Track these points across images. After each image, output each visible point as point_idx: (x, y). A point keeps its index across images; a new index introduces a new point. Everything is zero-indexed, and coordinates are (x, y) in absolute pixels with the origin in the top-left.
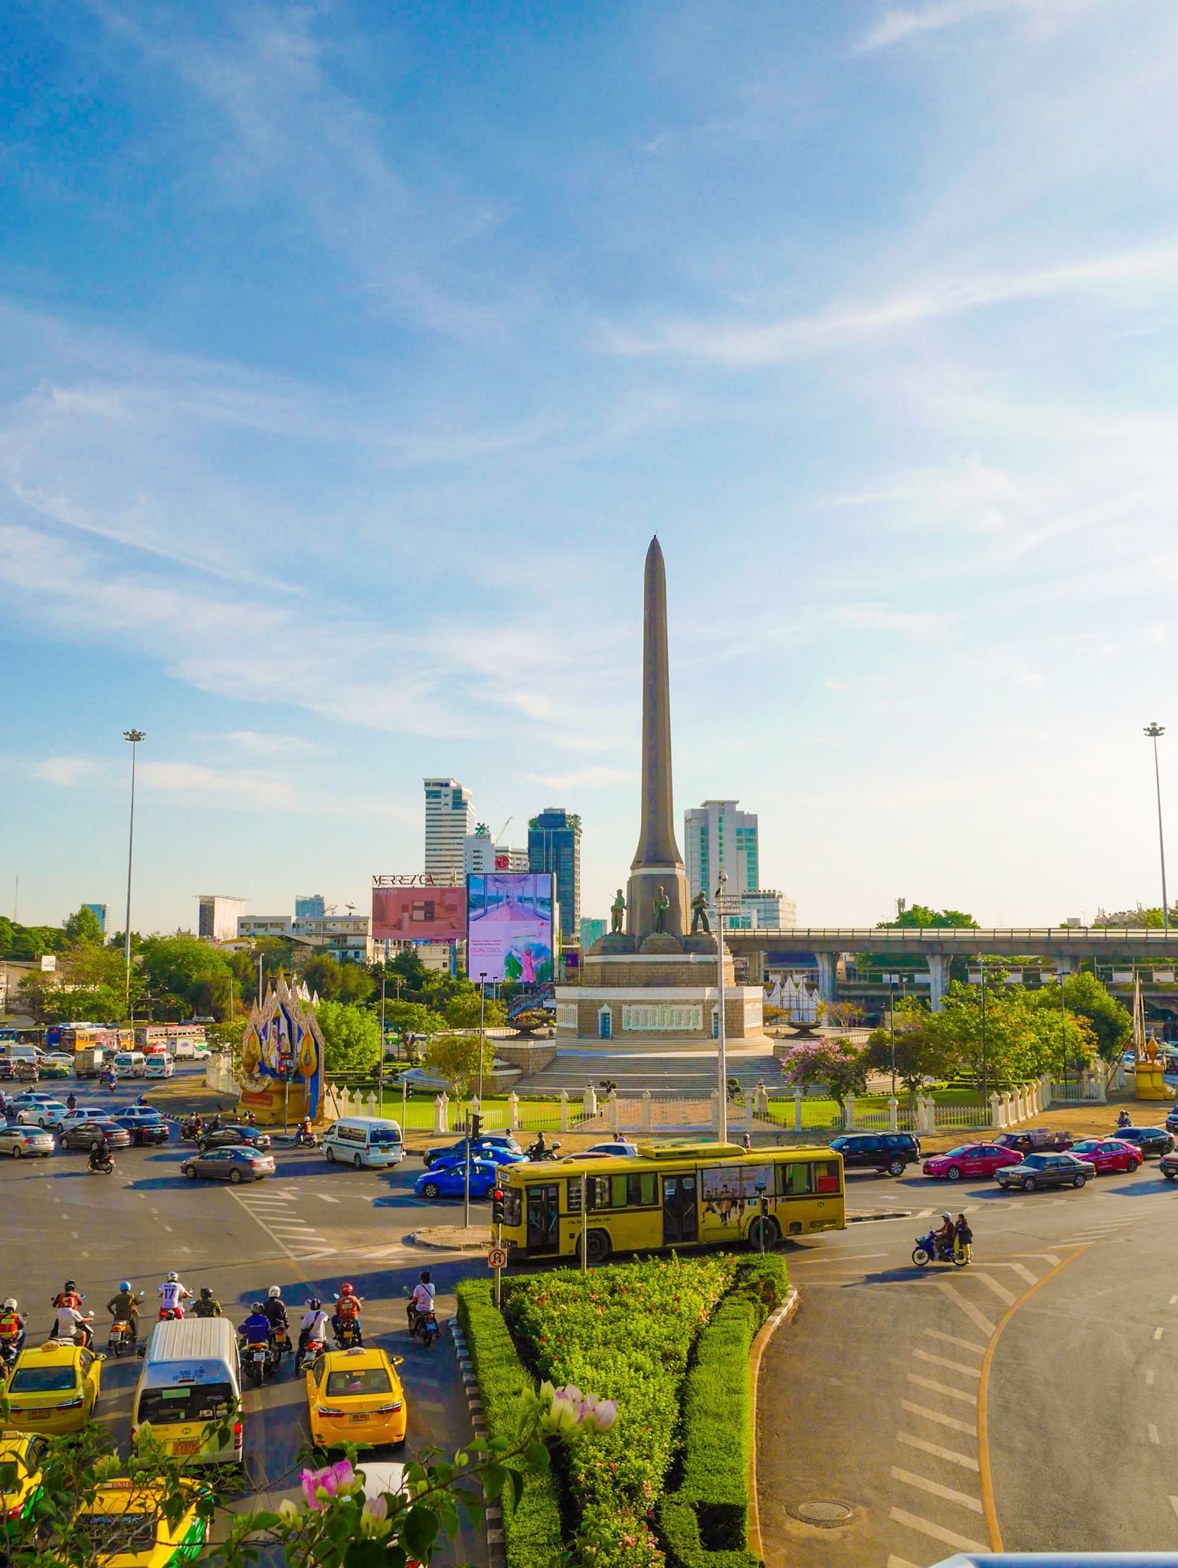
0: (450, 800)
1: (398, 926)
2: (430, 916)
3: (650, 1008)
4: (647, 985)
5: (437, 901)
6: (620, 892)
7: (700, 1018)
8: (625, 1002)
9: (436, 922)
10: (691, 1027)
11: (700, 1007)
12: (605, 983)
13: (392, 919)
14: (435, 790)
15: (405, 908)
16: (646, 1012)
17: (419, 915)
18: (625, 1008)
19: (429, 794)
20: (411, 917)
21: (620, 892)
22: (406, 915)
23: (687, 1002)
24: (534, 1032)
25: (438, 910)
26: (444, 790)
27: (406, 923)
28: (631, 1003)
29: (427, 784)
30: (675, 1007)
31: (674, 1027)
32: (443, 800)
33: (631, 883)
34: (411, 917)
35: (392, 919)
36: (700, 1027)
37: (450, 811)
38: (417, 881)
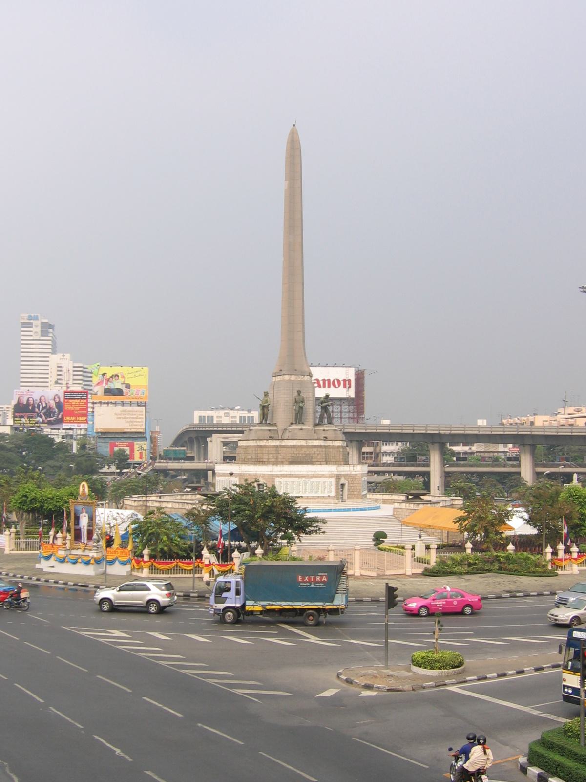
0: (38, 330)
3: (296, 480)
4: (292, 463)
6: (266, 394)
7: (333, 488)
8: (277, 476)
10: (326, 494)
11: (333, 480)
12: (259, 461)
16: (293, 483)
18: (277, 480)
23: (323, 476)
26: (35, 322)
28: (282, 476)
30: (314, 480)
31: (314, 494)
32: (34, 329)
36: (333, 494)
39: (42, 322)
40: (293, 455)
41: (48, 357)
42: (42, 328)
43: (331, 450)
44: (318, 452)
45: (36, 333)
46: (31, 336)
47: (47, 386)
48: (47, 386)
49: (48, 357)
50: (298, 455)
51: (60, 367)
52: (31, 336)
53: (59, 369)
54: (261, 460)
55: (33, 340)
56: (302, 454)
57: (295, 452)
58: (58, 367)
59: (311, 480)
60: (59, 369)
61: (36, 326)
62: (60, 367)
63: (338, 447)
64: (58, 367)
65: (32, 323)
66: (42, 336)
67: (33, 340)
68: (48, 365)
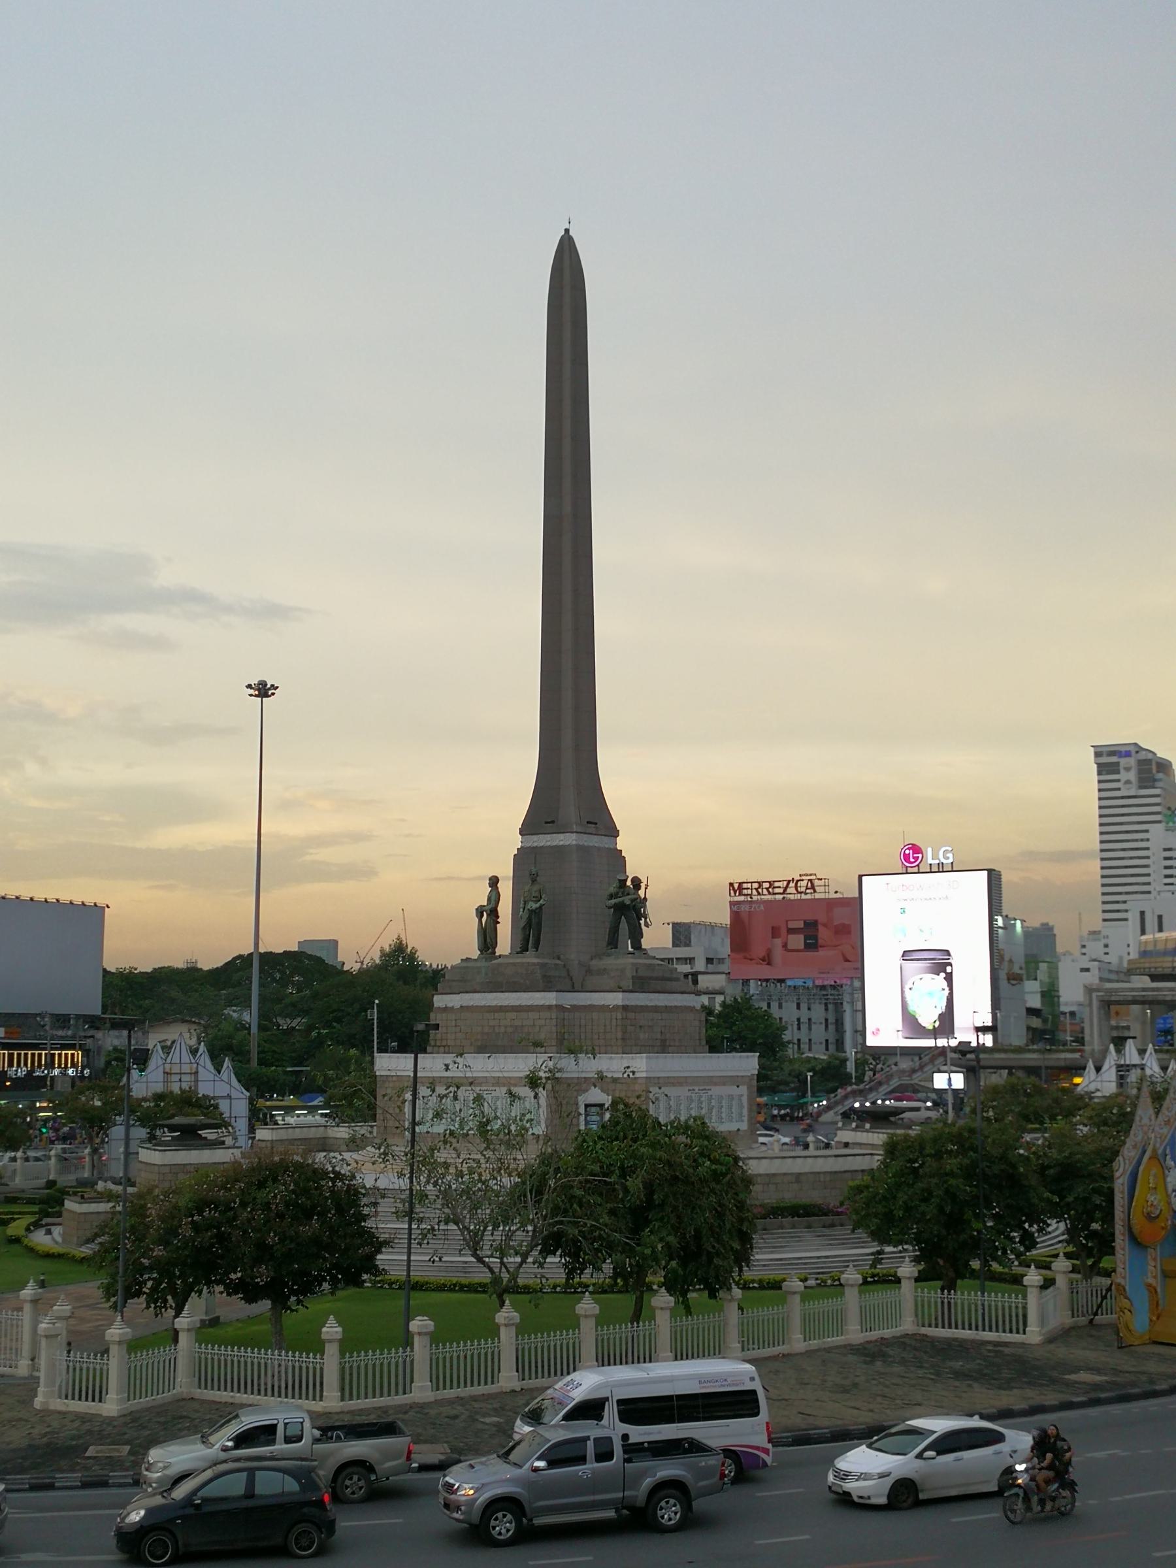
0: (1132, 776)
1: (768, 960)
2: (812, 944)
5: (822, 917)
6: (494, 882)
9: (822, 953)
13: (759, 951)
14: (1109, 761)
15: (775, 933)
17: (797, 941)
19: (1102, 769)
20: (785, 946)
21: (494, 882)
22: (778, 942)
24: (203, 1133)
25: (824, 934)
26: (1123, 762)
27: (778, 954)
29: (1098, 754)
32: (1123, 776)
33: (521, 858)
34: (785, 946)
35: (759, 951)
37: (1132, 793)
38: (791, 890)
39: (1139, 761)
40: (486, 1030)
41: (1147, 831)
42: (1140, 772)
43: (595, 1015)
44: (542, 1022)
45: (1128, 782)
46: (1119, 789)
47: (1149, 892)
48: (1149, 892)
49: (1147, 831)
50: (497, 1030)
51: (1170, 849)
52: (1119, 789)
53: (1168, 854)
54: (444, 1043)
55: (1122, 798)
56: (506, 1027)
57: (492, 1023)
58: (1165, 850)
59: (494, 1094)
60: (1168, 854)
61: (1128, 769)
62: (1170, 849)
63: (616, 1007)
64: (1165, 850)
65: (1118, 764)
66: (1141, 787)
67: (1122, 798)
68: (1148, 849)
